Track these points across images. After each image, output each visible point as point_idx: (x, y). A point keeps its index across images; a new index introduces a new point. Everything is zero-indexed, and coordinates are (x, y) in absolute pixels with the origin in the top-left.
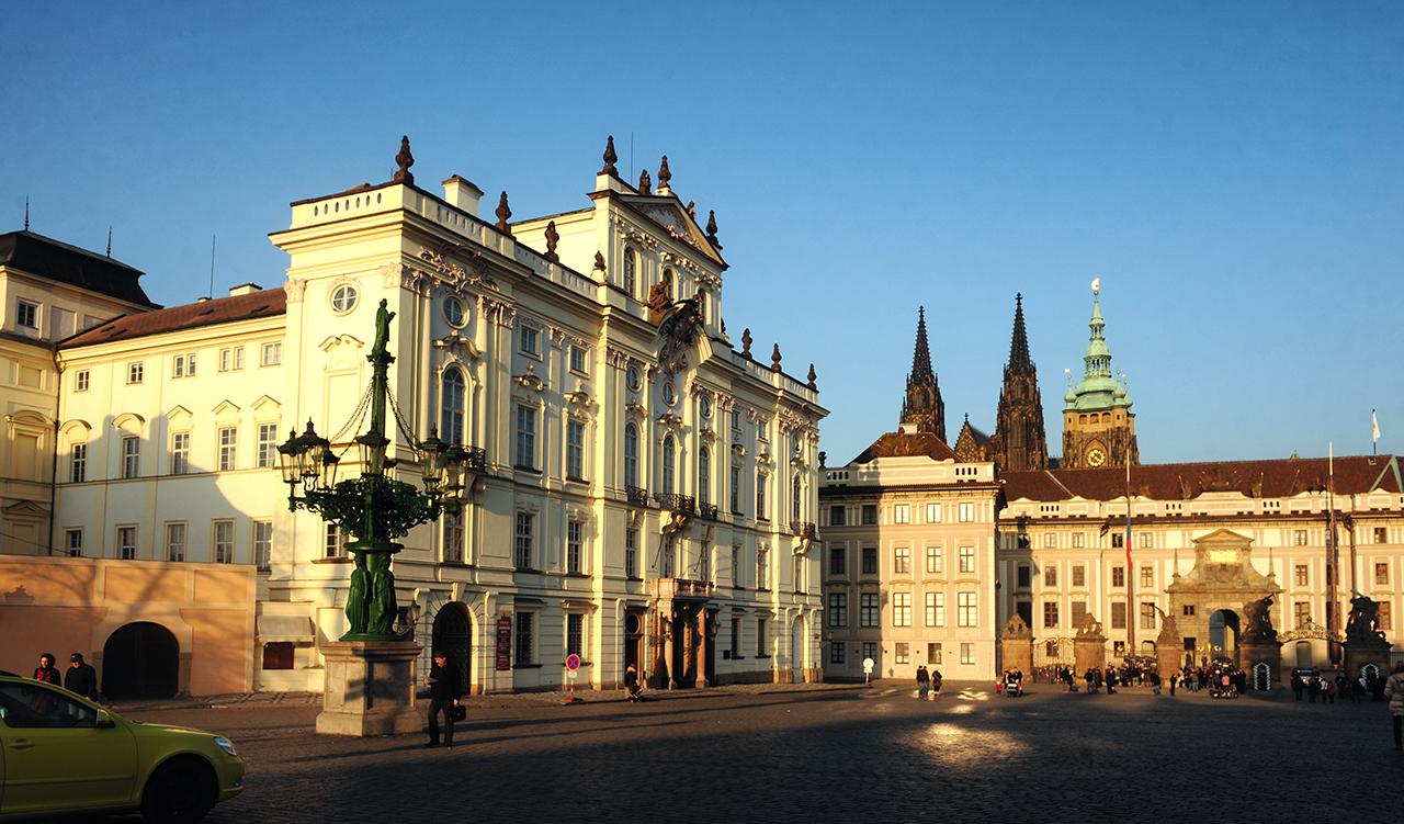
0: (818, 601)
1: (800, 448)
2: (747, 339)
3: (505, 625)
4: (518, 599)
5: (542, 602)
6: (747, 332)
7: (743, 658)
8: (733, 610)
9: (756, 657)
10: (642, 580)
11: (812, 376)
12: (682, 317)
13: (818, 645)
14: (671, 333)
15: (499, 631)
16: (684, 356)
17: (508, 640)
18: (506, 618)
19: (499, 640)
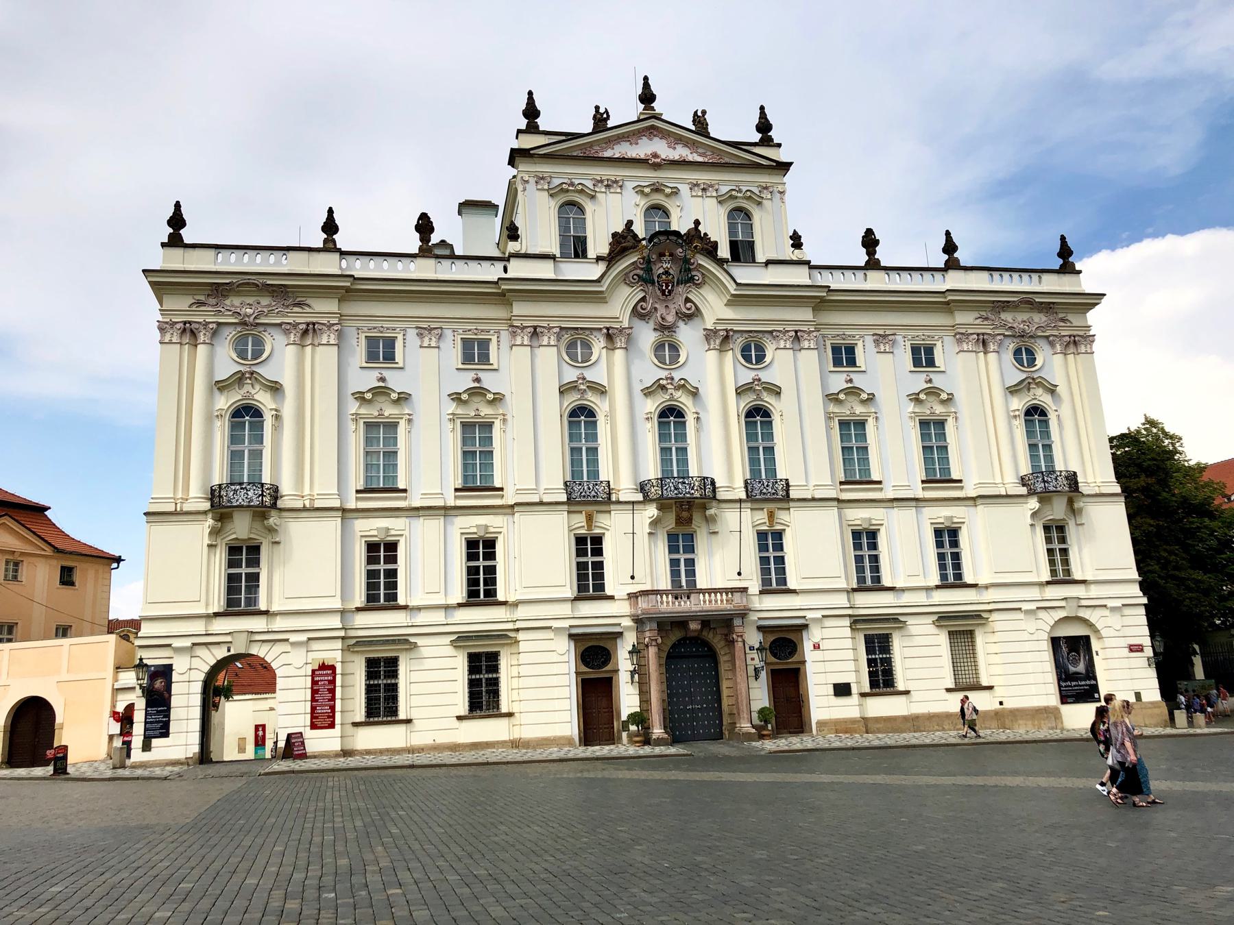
0: (1135, 590)
1: (1039, 362)
2: (870, 241)
3: (327, 675)
4: (353, 644)
6: (869, 232)
7: (907, 693)
8: (855, 622)
9: (948, 690)
10: (612, 598)
12: (662, 255)
13: (1144, 662)
15: (314, 683)
16: (688, 300)
17: (332, 691)
18: (327, 668)
19: (314, 692)
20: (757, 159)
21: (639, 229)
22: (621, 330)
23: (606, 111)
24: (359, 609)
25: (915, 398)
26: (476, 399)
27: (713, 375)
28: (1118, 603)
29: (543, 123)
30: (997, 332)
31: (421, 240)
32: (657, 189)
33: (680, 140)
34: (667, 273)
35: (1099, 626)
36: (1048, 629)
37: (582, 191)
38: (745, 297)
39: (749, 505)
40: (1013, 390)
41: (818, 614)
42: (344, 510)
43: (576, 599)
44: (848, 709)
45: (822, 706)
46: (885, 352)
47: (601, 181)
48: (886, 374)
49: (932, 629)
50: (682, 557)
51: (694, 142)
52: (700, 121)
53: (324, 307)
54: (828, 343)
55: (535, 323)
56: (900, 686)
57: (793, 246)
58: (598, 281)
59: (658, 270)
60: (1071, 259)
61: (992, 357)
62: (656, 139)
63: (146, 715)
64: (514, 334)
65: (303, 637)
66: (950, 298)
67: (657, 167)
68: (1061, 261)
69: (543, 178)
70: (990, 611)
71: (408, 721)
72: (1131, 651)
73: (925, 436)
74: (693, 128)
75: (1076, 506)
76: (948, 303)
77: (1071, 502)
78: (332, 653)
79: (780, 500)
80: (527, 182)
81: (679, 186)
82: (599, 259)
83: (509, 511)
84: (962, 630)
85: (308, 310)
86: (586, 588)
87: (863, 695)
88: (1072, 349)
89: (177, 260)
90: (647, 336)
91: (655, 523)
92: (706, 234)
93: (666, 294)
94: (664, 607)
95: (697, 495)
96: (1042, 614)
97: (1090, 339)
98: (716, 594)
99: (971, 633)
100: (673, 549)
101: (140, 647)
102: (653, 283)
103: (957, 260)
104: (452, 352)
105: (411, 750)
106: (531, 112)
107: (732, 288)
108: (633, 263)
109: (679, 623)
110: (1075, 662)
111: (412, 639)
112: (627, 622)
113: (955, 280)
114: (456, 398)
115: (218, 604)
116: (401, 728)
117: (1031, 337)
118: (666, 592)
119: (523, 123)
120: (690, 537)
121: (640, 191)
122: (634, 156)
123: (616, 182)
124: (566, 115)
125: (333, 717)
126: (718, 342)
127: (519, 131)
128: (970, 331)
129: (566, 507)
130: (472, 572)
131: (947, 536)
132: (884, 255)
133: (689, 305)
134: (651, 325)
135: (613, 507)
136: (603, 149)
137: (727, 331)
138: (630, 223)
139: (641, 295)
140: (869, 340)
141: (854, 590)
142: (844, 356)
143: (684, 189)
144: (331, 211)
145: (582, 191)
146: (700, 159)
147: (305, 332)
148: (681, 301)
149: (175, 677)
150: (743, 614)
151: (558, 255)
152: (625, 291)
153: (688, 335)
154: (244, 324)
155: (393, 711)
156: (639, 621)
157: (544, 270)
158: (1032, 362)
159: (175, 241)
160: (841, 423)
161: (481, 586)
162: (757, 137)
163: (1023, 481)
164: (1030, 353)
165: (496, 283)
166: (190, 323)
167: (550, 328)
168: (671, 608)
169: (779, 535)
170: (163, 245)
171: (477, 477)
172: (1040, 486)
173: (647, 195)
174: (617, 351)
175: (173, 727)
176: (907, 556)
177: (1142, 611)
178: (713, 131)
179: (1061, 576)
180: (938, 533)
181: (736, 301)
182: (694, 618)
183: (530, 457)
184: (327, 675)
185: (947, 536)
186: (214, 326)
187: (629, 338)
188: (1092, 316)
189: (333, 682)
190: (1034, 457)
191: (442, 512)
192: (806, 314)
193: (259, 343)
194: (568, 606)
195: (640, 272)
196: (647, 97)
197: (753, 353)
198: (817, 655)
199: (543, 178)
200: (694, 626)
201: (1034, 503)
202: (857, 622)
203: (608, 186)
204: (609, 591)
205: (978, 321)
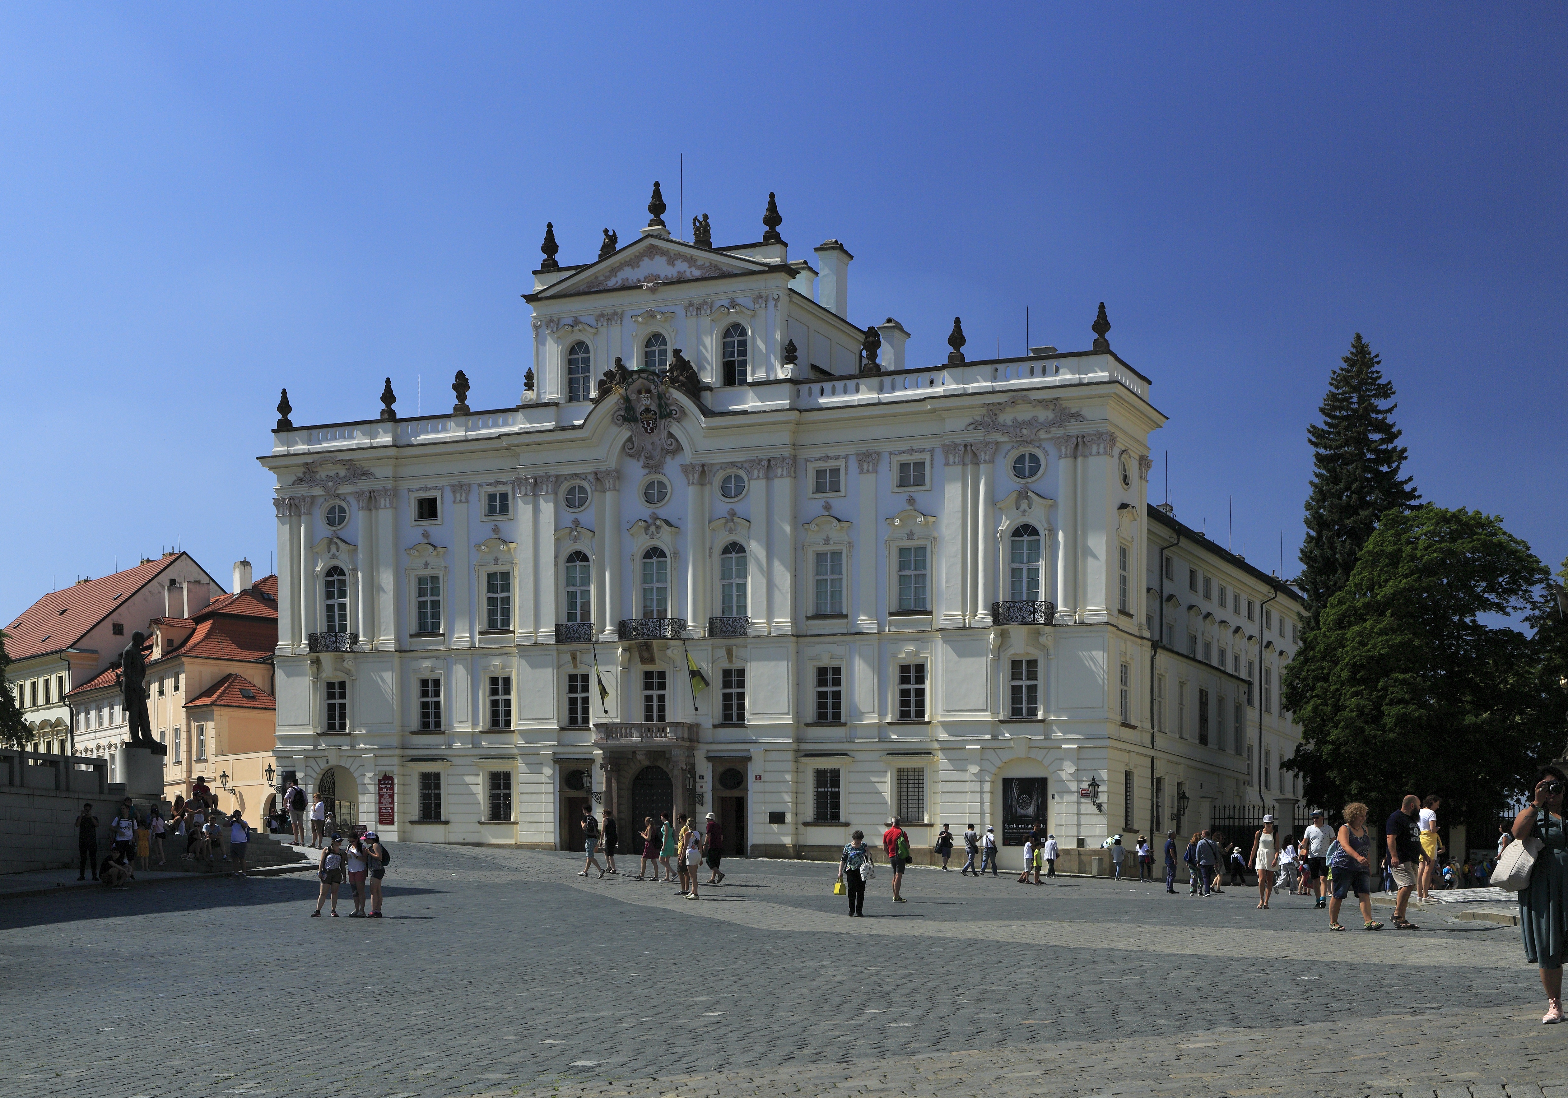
12: (640, 392)
16: (671, 435)
22: (608, 473)
34: (647, 410)
50: (655, 693)
56: (842, 820)
90: (636, 472)
100: (648, 686)
110: (1025, 805)
118: (639, 726)
120: (662, 675)
137: (703, 466)
138: (618, 360)
147: (370, 497)
148: (665, 435)
153: (672, 468)
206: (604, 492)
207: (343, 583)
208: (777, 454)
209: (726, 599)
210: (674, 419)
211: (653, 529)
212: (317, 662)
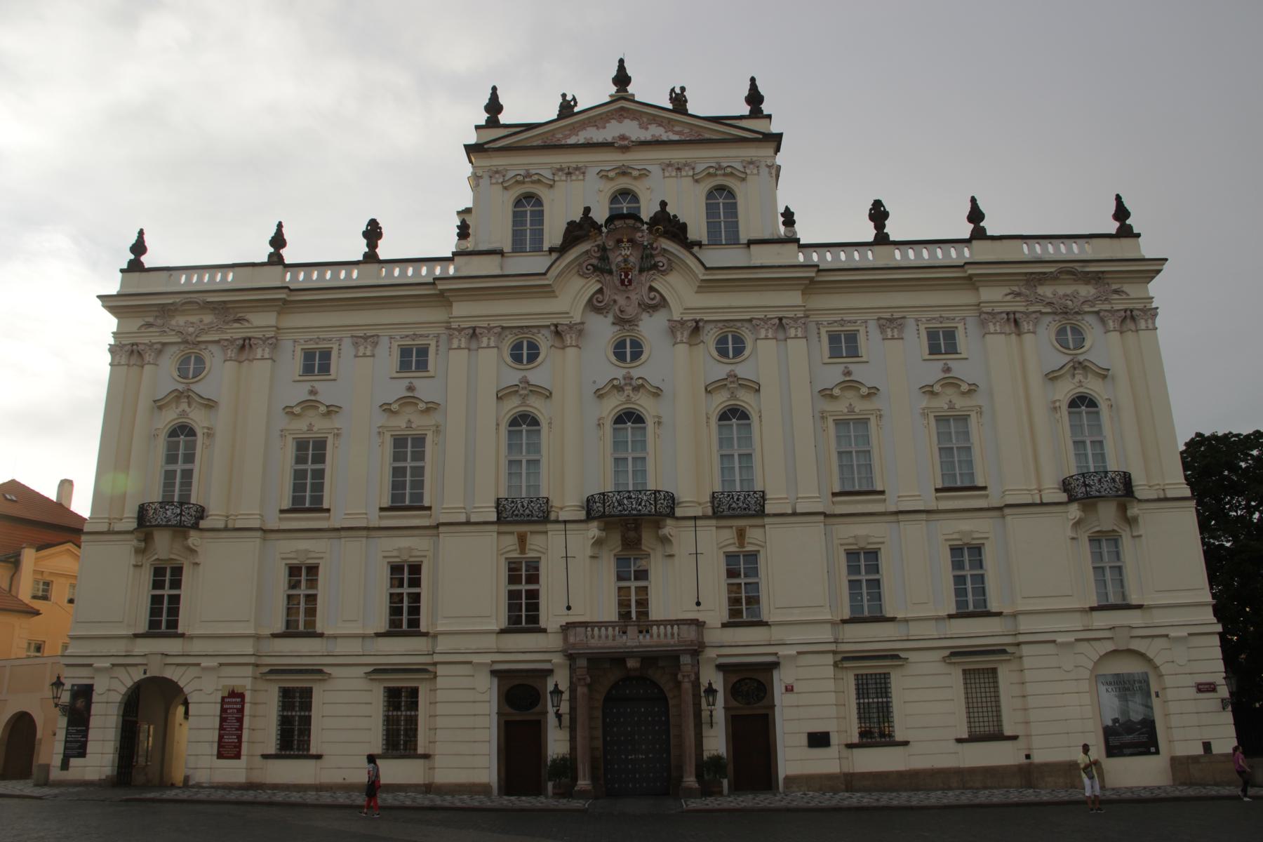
1: (1087, 344)
3: (236, 703)
5: (320, 672)
6: (877, 204)
7: (906, 743)
9: (959, 741)
10: (544, 631)
11: (1121, 213)
12: (619, 241)
14: (601, 267)
15: (223, 710)
16: (652, 289)
17: (240, 720)
20: (750, 133)
21: (600, 214)
22: (571, 326)
23: (574, 99)
24: (275, 636)
25: (929, 391)
26: (409, 409)
27: (678, 372)
28: (1183, 632)
29: (503, 118)
30: (1032, 309)
31: (368, 245)
32: (624, 172)
33: (655, 120)
34: (626, 261)
35: (1158, 661)
36: (1091, 665)
37: (539, 181)
38: (716, 281)
39: (714, 522)
40: (1052, 377)
41: (792, 651)
42: (264, 531)
43: (503, 631)
44: (826, 762)
45: (793, 759)
46: (893, 338)
47: (561, 169)
48: (896, 365)
49: (943, 668)
50: (633, 584)
51: (670, 120)
52: (679, 100)
53: (262, 320)
54: (823, 331)
55: (473, 324)
56: (899, 737)
57: (784, 223)
58: (544, 274)
59: (616, 258)
60: (1128, 222)
61: (1028, 338)
62: (627, 121)
63: (67, 733)
64: (450, 337)
65: (213, 663)
66: (970, 272)
67: (625, 149)
68: (1117, 224)
69: (497, 172)
70: (1018, 644)
71: (319, 757)
72: (1199, 691)
73: (943, 436)
74: (670, 106)
75: (1130, 513)
76: (970, 277)
77: (1123, 509)
78: (242, 679)
79: (752, 516)
80: (481, 177)
81: (648, 168)
82: (551, 250)
83: (434, 532)
84: (980, 670)
85: (247, 325)
86: (517, 620)
87: (850, 746)
88: (1131, 325)
89: (142, 284)
90: (603, 330)
91: (598, 543)
92: (675, 216)
93: (626, 283)
94: (593, 642)
95: (645, 511)
96: (1083, 647)
97: (1153, 313)
98: (658, 626)
99: (994, 671)
101: (68, 665)
102: (610, 272)
103: (984, 229)
104: (388, 358)
105: (319, 788)
106: (494, 107)
107: (701, 274)
108: (587, 252)
109: (618, 660)
111: (326, 670)
112: (557, 659)
113: (983, 251)
114: (386, 408)
115: (143, 627)
116: (312, 763)
117: (1077, 313)
119: (482, 118)
121: (603, 175)
122: (600, 140)
123: (577, 169)
124: (529, 106)
125: (239, 747)
126: (686, 334)
127: (477, 127)
128: (997, 310)
129: (495, 528)
130: (395, 599)
131: (967, 556)
132: (894, 230)
133: (652, 295)
134: (610, 319)
135: (550, 527)
136: (566, 137)
137: (697, 322)
138: (587, 210)
139: (599, 286)
140: (872, 325)
141: (844, 622)
142: (844, 344)
143: (655, 170)
144: (280, 225)
145: (539, 181)
146: (676, 138)
147: (243, 347)
148: (645, 290)
149: (95, 698)
150: (697, 650)
151: (507, 248)
152: (577, 283)
153: (651, 328)
154: (186, 342)
155: (305, 744)
156: (571, 657)
157: (488, 266)
158: (1080, 343)
159: (135, 266)
160: (837, 422)
161: (405, 616)
162: (745, 110)
163: (1066, 486)
164: (1077, 331)
165: (434, 284)
166: (137, 344)
167: (489, 329)
168: (610, 643)
169: (753, 557)
170: (122, 271)
171: (406, 495)
172: (1081, 491)
173: (612, 179)
174: (568, 350)
175: (91, 747)
176: (917, 580)
177: (1216, 641)
178: (692, 108)
179: (1112, 600)
180: (956, 551)
181: (706, 286)
182: (632, 654)
183: (467, 473)
184: (236, 703)
185: (967, 556)
186: (159, 346)
187: (580, 333)
188: (1156, 288)
189: (241, 711)
190: (1081, 456)
191: (364, 533)
192: (793, 298)
193: (200, 360)
194: (494, 636)
195: (594, 261)
196: (622, 79)
197: (731, 346)
198: (790, 699)
199: (497, 172)
200: (631, 663)
201: (1074, 511)
202: (844, 660)
203: (569, 174)
204: (542, 624)
205: (1009, 298)
206: (564, 348)
207: (191, 447)
208: (791, 315)
209: (726, 470)
210: (659, 271)
211: (628, 389)
212: (147, 539)
